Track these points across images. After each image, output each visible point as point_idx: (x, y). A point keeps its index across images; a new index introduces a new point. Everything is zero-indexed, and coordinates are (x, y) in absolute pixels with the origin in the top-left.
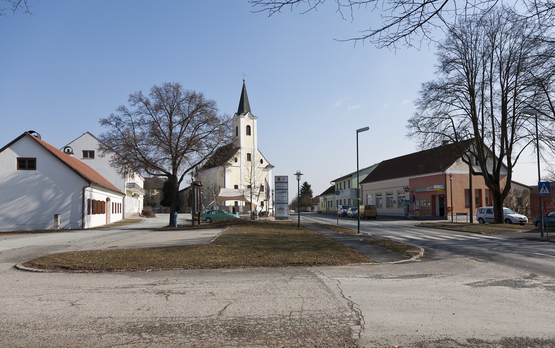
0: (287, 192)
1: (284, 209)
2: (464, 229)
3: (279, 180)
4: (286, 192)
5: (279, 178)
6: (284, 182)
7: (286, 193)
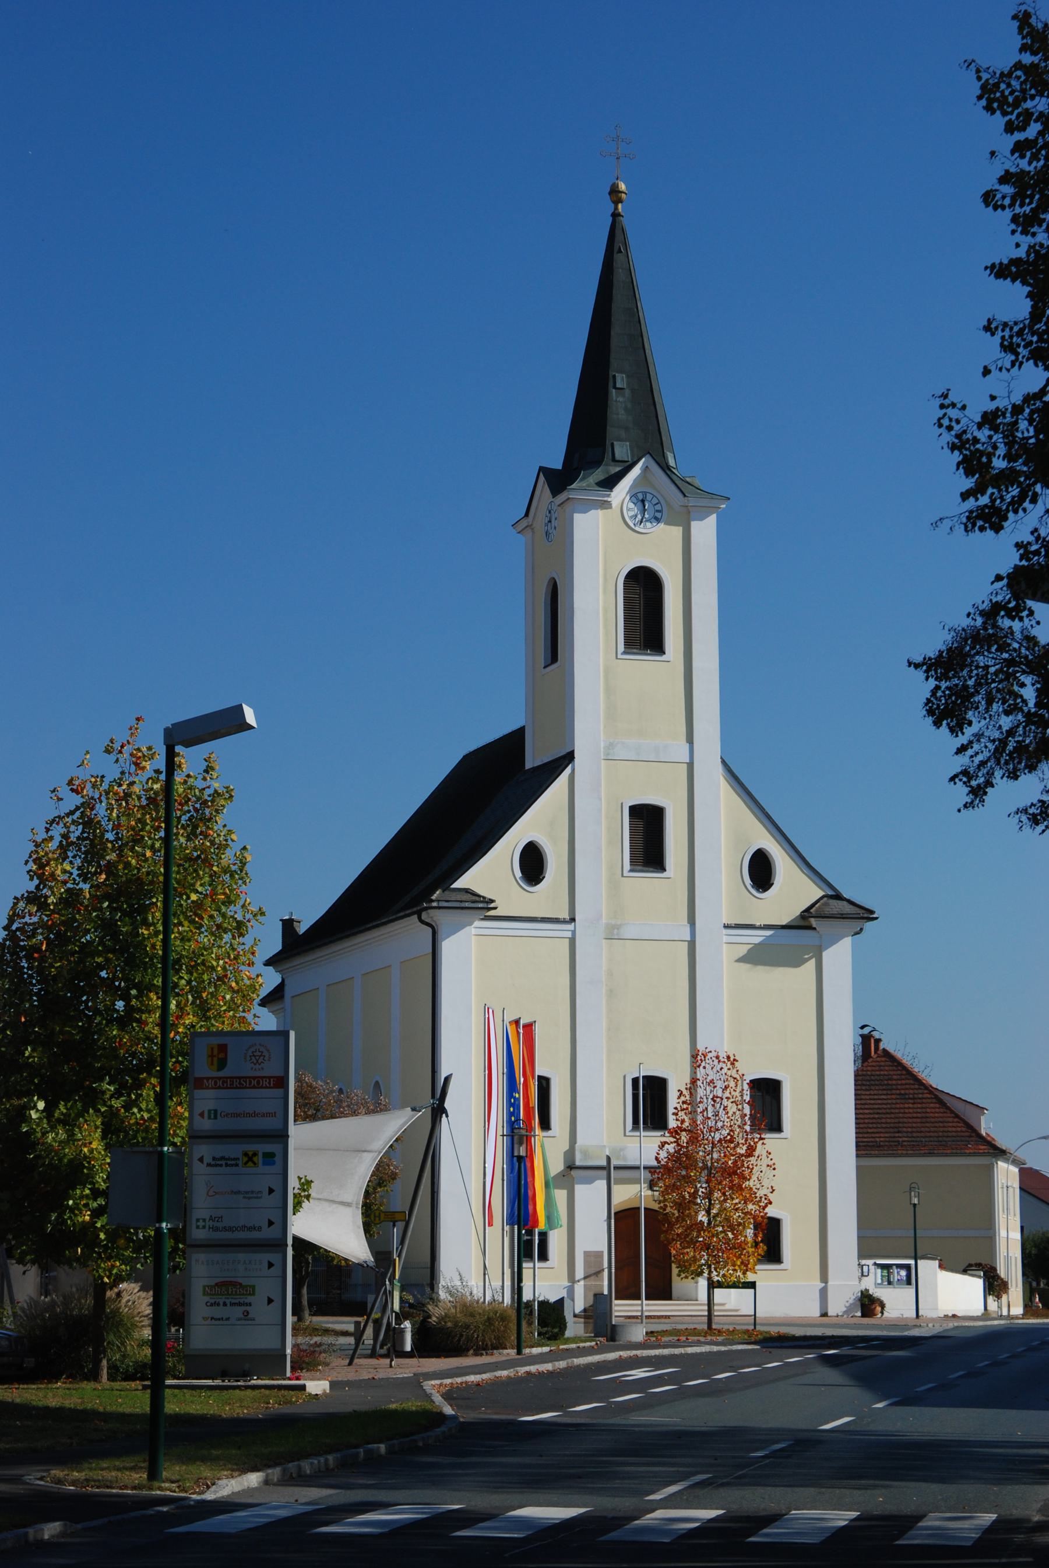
0: (278, 1159)
1: (251, 1290)
2: (827, 1341)
3: (222, 1064)
4: (269, 1157)
5: (223, 1048)
6: (257, 1082)
7: (267, 1169)
